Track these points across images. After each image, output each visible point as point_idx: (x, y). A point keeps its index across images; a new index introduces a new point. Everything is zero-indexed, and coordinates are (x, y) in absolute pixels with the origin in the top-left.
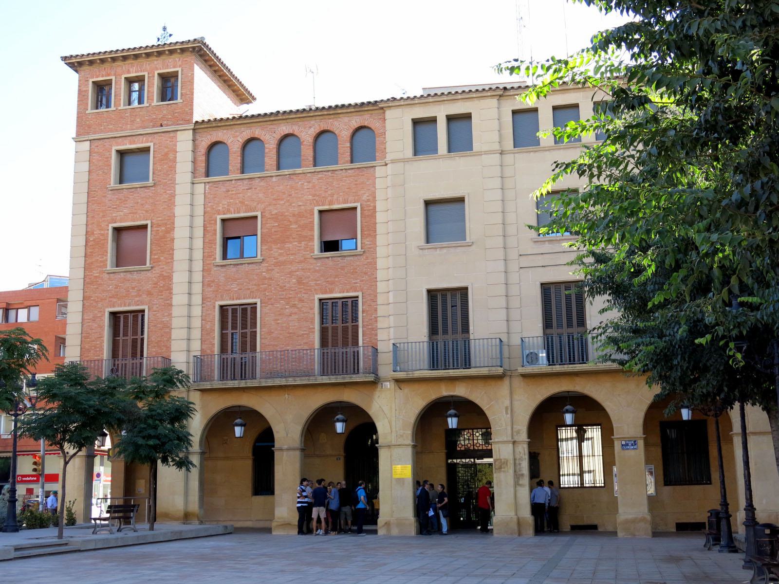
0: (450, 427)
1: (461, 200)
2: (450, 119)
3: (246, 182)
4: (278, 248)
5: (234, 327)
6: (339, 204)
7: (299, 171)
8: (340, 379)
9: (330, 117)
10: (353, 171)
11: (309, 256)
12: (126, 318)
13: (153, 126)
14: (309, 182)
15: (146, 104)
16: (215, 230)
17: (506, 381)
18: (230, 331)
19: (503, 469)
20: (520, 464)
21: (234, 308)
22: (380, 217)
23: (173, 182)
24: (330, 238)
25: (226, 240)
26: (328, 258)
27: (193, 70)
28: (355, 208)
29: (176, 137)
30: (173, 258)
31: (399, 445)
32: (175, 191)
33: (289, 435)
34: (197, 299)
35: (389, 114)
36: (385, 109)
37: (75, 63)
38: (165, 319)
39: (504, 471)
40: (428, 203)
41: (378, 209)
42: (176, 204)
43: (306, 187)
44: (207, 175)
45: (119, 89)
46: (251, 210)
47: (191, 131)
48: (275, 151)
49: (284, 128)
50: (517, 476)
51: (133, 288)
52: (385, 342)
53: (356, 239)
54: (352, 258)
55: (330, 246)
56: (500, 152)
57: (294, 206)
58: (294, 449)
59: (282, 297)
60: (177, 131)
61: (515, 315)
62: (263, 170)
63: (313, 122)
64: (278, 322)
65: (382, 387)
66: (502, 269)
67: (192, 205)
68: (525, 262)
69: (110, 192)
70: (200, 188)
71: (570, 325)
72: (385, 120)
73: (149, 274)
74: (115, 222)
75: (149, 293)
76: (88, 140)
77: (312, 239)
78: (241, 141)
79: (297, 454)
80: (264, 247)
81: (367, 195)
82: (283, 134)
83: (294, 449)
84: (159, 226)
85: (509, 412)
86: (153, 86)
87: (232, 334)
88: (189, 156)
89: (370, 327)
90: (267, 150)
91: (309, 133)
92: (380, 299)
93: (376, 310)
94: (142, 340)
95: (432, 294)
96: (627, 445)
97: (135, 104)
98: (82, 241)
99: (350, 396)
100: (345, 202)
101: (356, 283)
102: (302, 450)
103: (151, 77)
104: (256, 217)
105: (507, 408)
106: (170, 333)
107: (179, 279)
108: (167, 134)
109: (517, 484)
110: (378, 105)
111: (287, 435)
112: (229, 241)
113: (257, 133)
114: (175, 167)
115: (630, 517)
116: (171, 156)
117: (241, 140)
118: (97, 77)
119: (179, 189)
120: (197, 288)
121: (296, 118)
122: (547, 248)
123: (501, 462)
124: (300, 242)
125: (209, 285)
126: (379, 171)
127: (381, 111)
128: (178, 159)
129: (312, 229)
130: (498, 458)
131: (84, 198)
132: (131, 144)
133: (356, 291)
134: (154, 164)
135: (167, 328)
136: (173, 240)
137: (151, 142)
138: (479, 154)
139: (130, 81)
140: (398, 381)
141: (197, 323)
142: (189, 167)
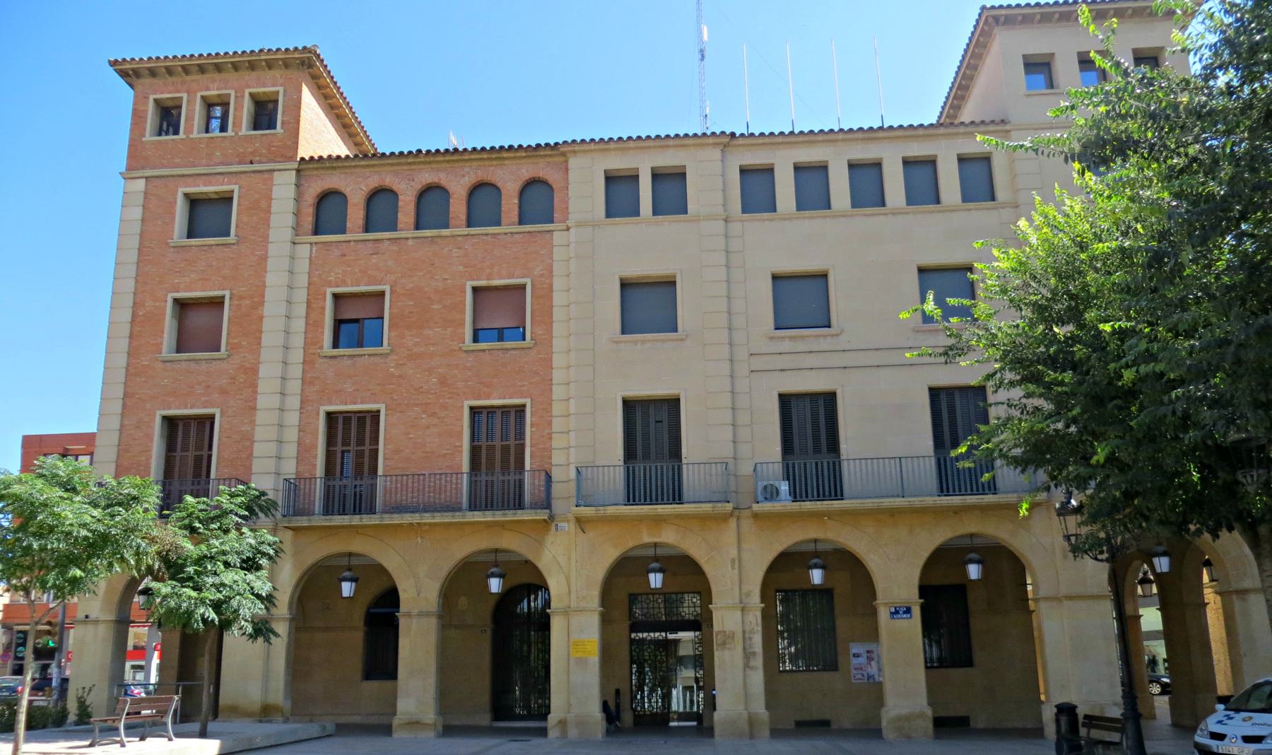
0: (653, 586)
3: (370, 245)
4: (412, 336)
5: (346, 442)
6: (501, 278)
7: (445, 232)
9: (491, 163)
10: (521, 236)
11: (457, 348)
13: (240, 163)
14: (460, 248)
15: (230, 133)
16: (323, 308)
17: (733, 523)
18: (339, 448)
19: (727, 646)
20: (750, 639)
21: (347, 416)
22: (558, 298)
23: (266, 239)
25: (338, 323)
26: (484, 350)
27: (300, 91)
29: (272, 179)
30: (259, 344)
32: (267, 252)
34: (294, 402)
36: (568, 155)
37: (129, 72)
38: (246, 428)
39: (729, 649)
40: (625, 285)
41: (555, 287)
42: (268, 270)
43: (456, 255)
44: (316, 232)
45: (191, 115)
47: (294, 172)
49: (427, 175)
50: (748, 655)
51: (199, 383)
53: (524, 328)
54: (517, 352)
56: (724, 217)
57: (437, 280)
58: (428, 614)
59: (417, 402)
60: (274, 170)
61: (744, 434)
64: (411, 436)
65: (557, 530)
66: (728, 372)
68: (757, 363)
69: (172, 249)
70: (304, 251)
71: (817, 450)
72: (567, 169)
73: (224, 365)
74: (178, 292)
75: (223, 392)
76: (142, 177)
77: (462, 324)
79: (433, 623)
80: (393, 334)
81: (541, 268)
82: (424, 183)
83: (428, 614)
84: (241, 298)
85: (737, 566)
86: (243, 112)
87: (343, 452)
88: (291, 206)
89: (541, 446)
90: (400, 204)
91: (461, 182)
92: (557, 409)
93: (550, 423)
94: (210, 457)
96: (897, 612)
101: (523, 386)
102: (440, 617)
103: (239, 98)
105: (733, 561)
106: (251, 447)
107: (268, 372)
109: (747, 666)
110: (558, 149)
111: (418, 595)
113: (388, 180)
115: (904, 711)
116: (263, 204)
117: (364, 189)
118: (162, 93)
119: (272, 250)
120: (295, 386)
121: (444, 161)
122: (787, 346)
125: (311, 383)
126: (558, 238)
127: (562, 159)
128: (273, 210)
129: (463, 312)
130: (721, 629)
132: (205, 186)
136: (261, 318)
137: (235, 184)
139: (209, 105)
140: (579, 521)
141: (292, 435)
142: (290, 220)
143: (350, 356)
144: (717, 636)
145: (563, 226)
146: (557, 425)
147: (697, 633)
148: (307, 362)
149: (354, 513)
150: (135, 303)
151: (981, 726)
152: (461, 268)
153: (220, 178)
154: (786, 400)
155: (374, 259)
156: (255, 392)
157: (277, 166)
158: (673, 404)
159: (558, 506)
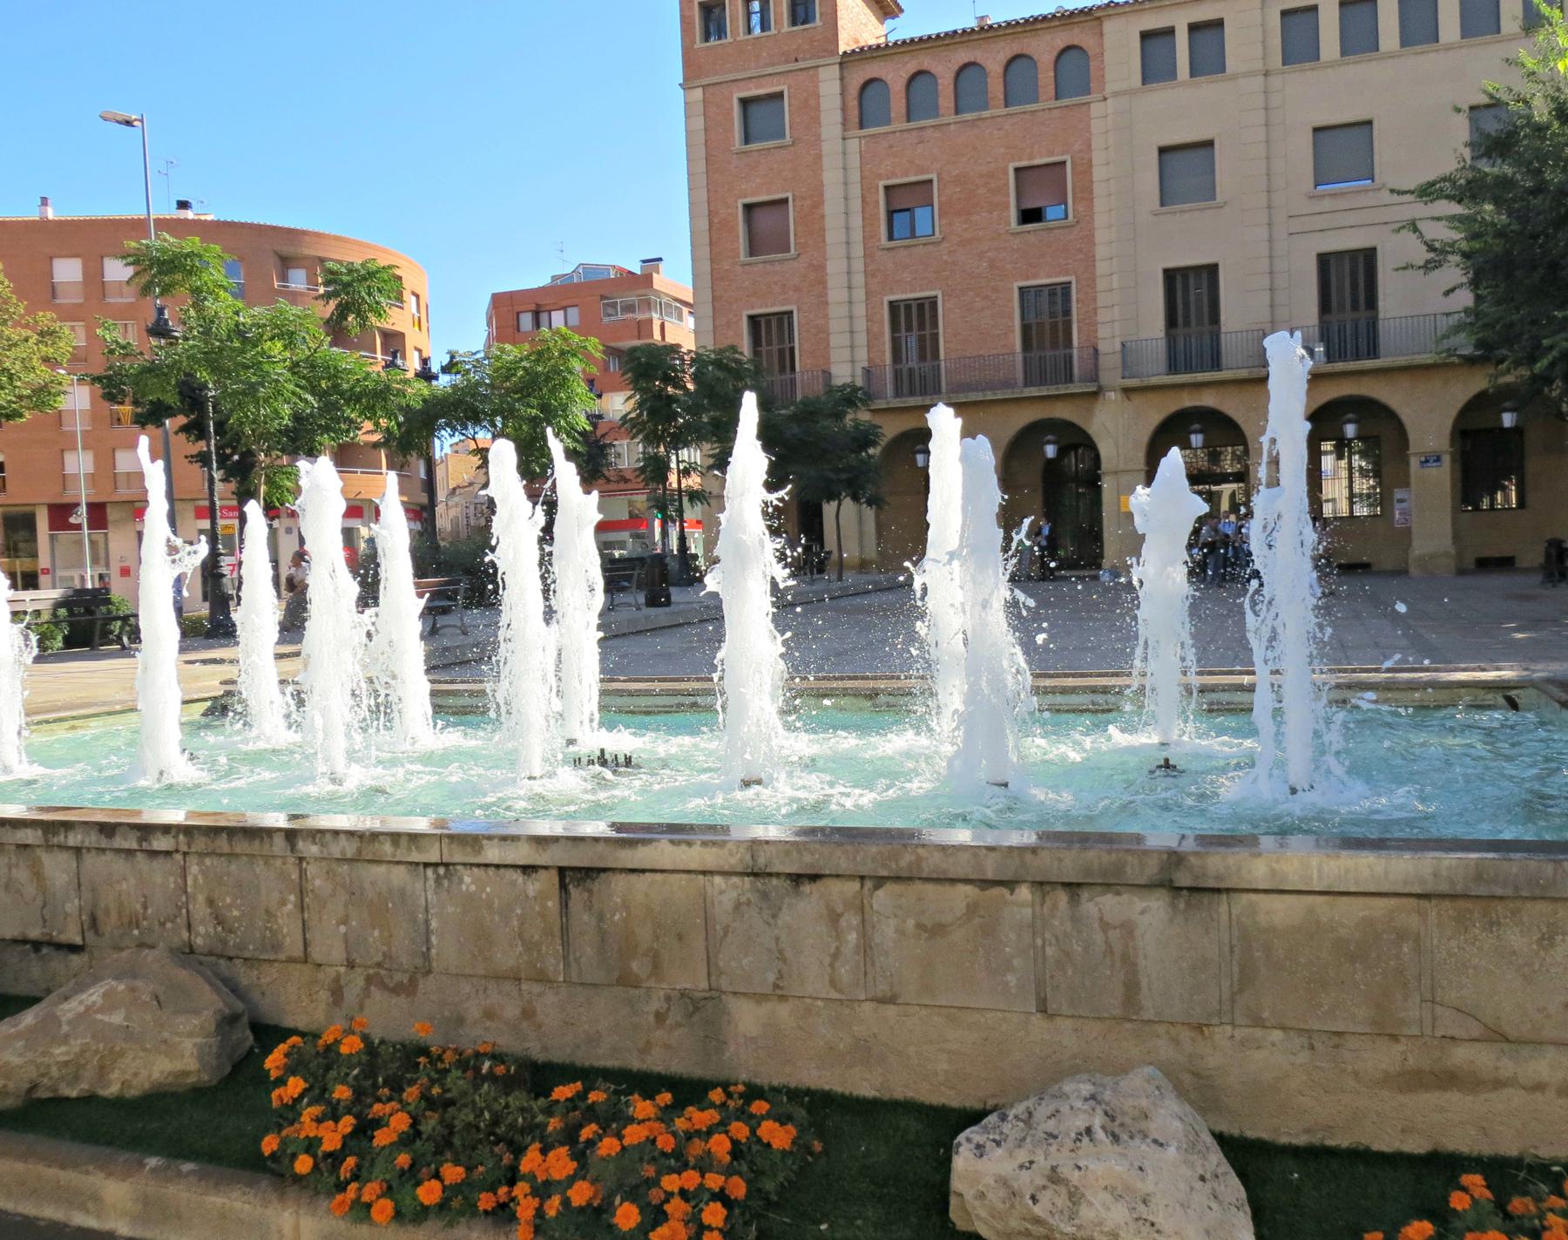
1: (1209, 144)
2: (1194, 28)
3: (914, 133)
5: (909, 328)
6: (1041, 157)
7: (986, 114)
8: (1053, 390)
12: (768, 323)
13: (787, 62)
15: (773, 31)
16: (877, 202)
18: (903, 333)
22: (1098, 173)
23: (818, 139)
24: (1030, 204)
25: (891, 213)
28: (1064, 163)
30: (824, 241)
34: (860, 294)
35: (1109, 26)
40: (1163, 151)
44: (861, 126)
46: (922, 172)
47: (837, 67)
48: (952, 87)
51: (775, 283)
52: (1109, 340)
53: (1066, 205)
55: (1030, 216)
62: (937, 115)
63: (1002, 44)
67: (845, 169)
70: (854, 145)
71: (1355, 307)
72: (1102, 34)
75: (797, 289)
77: (1007, 207)
78: (905, 75)
80: (944, 222)
84: (803, 198)
88: (837, 101)
90: (940, 88)
92: (1101, 284)
93: (1095, 299)
94: (792, 350)
95: (1170, 275)
96: (1427, 461)
97: (757, 31)
98: (704, 224)
99: (1063, 412)
100: (1051, 154)
104: (931, 181)
108: (805, 73)
112: (895, 215)
114: (818, 117)
116: (812, 102)
119: (826, 148)
120: (859, 279)
122: (1327, 204)
124: (990, 212)
125: (873, 276)
126: (1096, 109)
127: (1095, 23)
131: (701, 166)
132: (757, 88)
133: (1066, 275)
134: (790, 116)
135: (823, 333)
136: (823, 217)
138: (1234, 77)
140: (1127, 391)
141: (861, 325)
142: (838, 117)
143: (905, 247)
145: (1099, 96)
146: (1102, 299)
147: (1241, 485)
148: (868, 256)
149: (921, 395)
150: (710, 211)
151: (1526, 565)
152: (1002, 150)
153: (770, 78)
154: (1324, 261)
155: (920, 148)
156: (825, 288)
157: (821, 62)
158: (1210, 272)
159: (1105, 378)
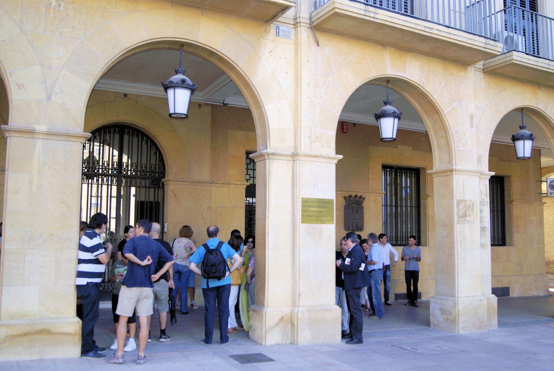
19: (468, 218)
31: (316, 156)
33: (53, 98)
39: (469, 222)
111: (49, 98)
123: (466, 205)
144: (458, 205)
